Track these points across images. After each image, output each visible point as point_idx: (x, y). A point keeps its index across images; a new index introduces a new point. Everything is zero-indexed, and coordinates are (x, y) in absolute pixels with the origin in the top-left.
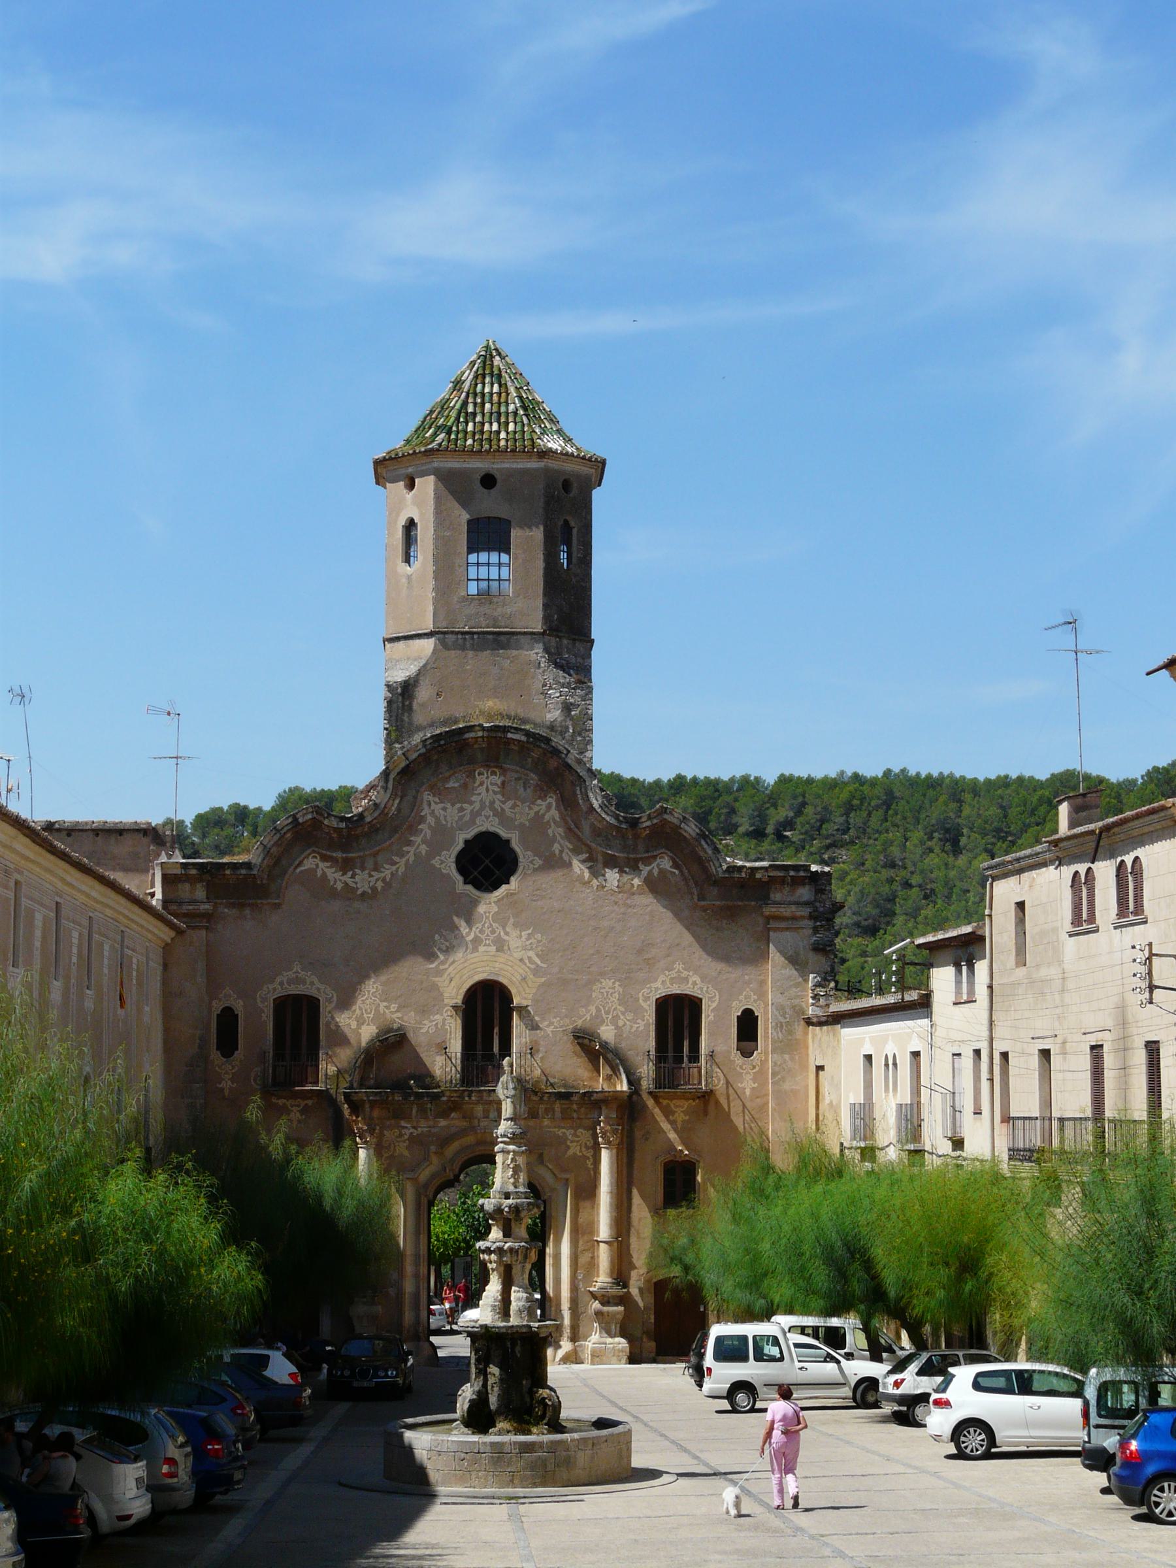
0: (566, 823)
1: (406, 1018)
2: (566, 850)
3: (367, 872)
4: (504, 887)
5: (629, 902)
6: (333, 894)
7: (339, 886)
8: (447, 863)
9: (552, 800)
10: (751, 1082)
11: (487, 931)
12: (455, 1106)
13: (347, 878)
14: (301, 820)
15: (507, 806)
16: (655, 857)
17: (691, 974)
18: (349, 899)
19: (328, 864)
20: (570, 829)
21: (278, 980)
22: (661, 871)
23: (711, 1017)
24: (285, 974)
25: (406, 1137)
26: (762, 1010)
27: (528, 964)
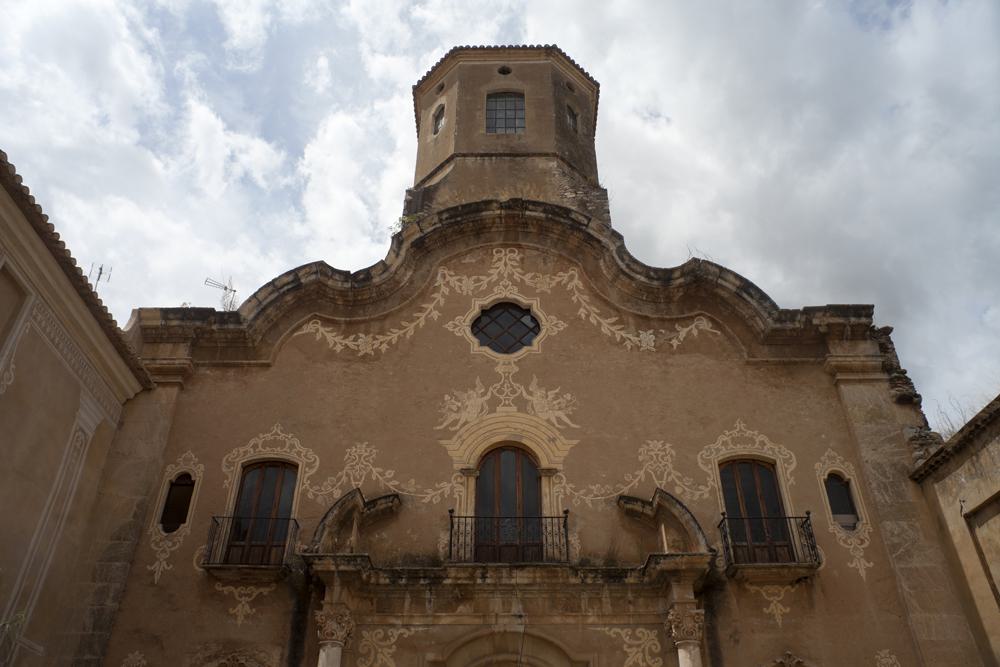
0: (591, 290)
1: (403, 486)
2: (593, 315)
3: (371, 335)
4: (525, 348)
5: (669, 361)
6: (331, 355)
7: (339, 348)
8: (462, 327)
9: (574, 272)
10: (863, 561)
11: (507, 391)
12: (464, 594)
13: (349, 342)
14: (303, 281)
15: (527, 278)
16: (692, 318)
17: (756, 432)
18: (349, 360)
19: (330, 329)
20: (597, 296)
21: (252, 442)
22: (701, 332)
23: (792, 480)
24: (261, 436)
25: (393, 640)
26: (853, 473)
27: (557, 425)
